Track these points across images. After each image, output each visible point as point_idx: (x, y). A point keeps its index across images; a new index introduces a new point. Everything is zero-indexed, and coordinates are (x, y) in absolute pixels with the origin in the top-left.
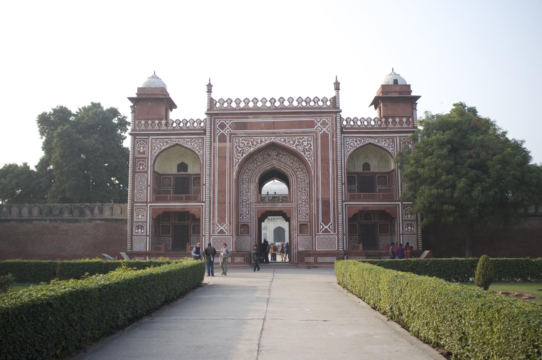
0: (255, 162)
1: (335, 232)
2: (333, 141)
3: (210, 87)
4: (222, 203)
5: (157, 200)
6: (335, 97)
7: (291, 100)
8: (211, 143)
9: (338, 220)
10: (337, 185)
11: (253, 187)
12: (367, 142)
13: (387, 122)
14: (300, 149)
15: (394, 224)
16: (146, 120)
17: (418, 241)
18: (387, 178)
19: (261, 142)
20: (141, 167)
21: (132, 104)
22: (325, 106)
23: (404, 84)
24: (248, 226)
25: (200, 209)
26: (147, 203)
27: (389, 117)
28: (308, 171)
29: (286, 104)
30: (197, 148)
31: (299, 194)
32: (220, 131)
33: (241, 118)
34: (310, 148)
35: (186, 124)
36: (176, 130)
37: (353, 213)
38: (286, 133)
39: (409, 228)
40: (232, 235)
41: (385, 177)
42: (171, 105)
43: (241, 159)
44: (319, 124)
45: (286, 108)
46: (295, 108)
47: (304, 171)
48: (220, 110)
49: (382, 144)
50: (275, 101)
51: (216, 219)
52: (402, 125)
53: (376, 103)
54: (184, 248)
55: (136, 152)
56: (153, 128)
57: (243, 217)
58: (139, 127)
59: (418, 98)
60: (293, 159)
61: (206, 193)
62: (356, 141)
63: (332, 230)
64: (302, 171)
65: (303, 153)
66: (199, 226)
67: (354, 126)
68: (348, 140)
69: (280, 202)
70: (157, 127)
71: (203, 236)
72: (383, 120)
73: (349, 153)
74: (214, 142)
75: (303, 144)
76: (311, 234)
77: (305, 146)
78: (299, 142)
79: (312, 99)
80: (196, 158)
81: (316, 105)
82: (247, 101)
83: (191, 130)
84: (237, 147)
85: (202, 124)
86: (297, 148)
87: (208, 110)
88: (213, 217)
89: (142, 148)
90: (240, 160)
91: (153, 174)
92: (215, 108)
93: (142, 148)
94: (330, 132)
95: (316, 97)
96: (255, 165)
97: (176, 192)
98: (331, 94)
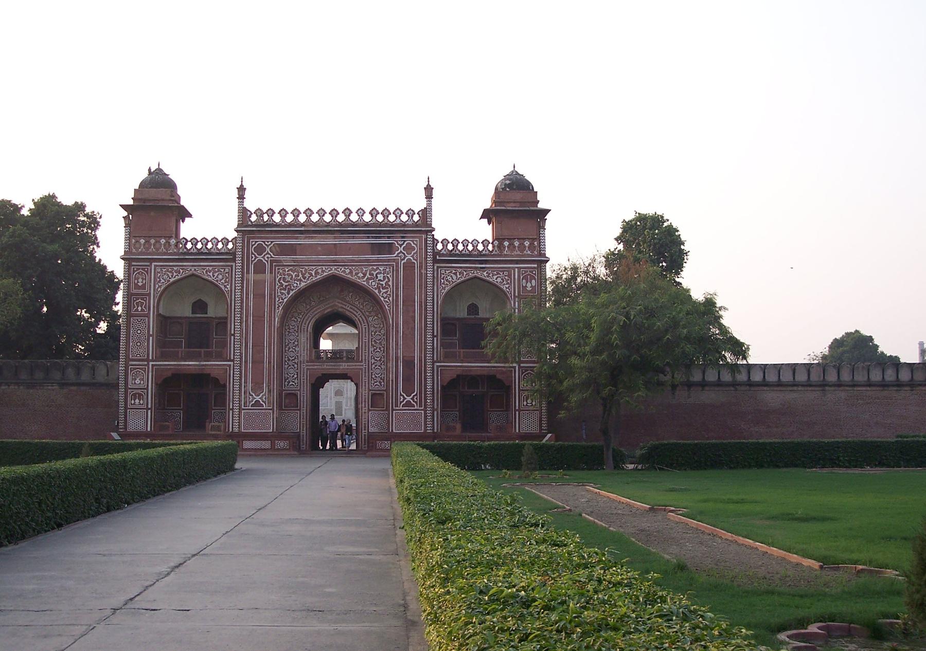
3: (241, 190)
4: (258, 362)
5: (163, 356)
8: (243, 275)
9: (426, 388)
11: (304, 339)
12: (471, 275)
13: (501, 246)
14: (372, 285)
16: (148, 238)
17: (541, 421)
20: (140, 308)
21: (125, 214)
24: (296, 395)
27: (504, 239)
28: (385, 318)
29: (354, 218)
32: (256, 257)
35: (207, 244)
36: (192, 254)
38: (353, 261)
42: (184, 214)
45: (354, 224)
49: (494, 279)
51: (250, 385)
52: (522, 251)
54: (201, 426)
55: (132, 285)
56: (157, 250)
58: (137, 249)
61: (235, 347)
65: (376, 291)
71: (230, 409)
74: (248, 272)
76: (387, 409)
81: (398, 221)
85: (230, 246)
86: (368, 283)
87: (239, 225)
89: (140, 280)
93: (140, 280)
97: (189, 346)
98: (419, 204)
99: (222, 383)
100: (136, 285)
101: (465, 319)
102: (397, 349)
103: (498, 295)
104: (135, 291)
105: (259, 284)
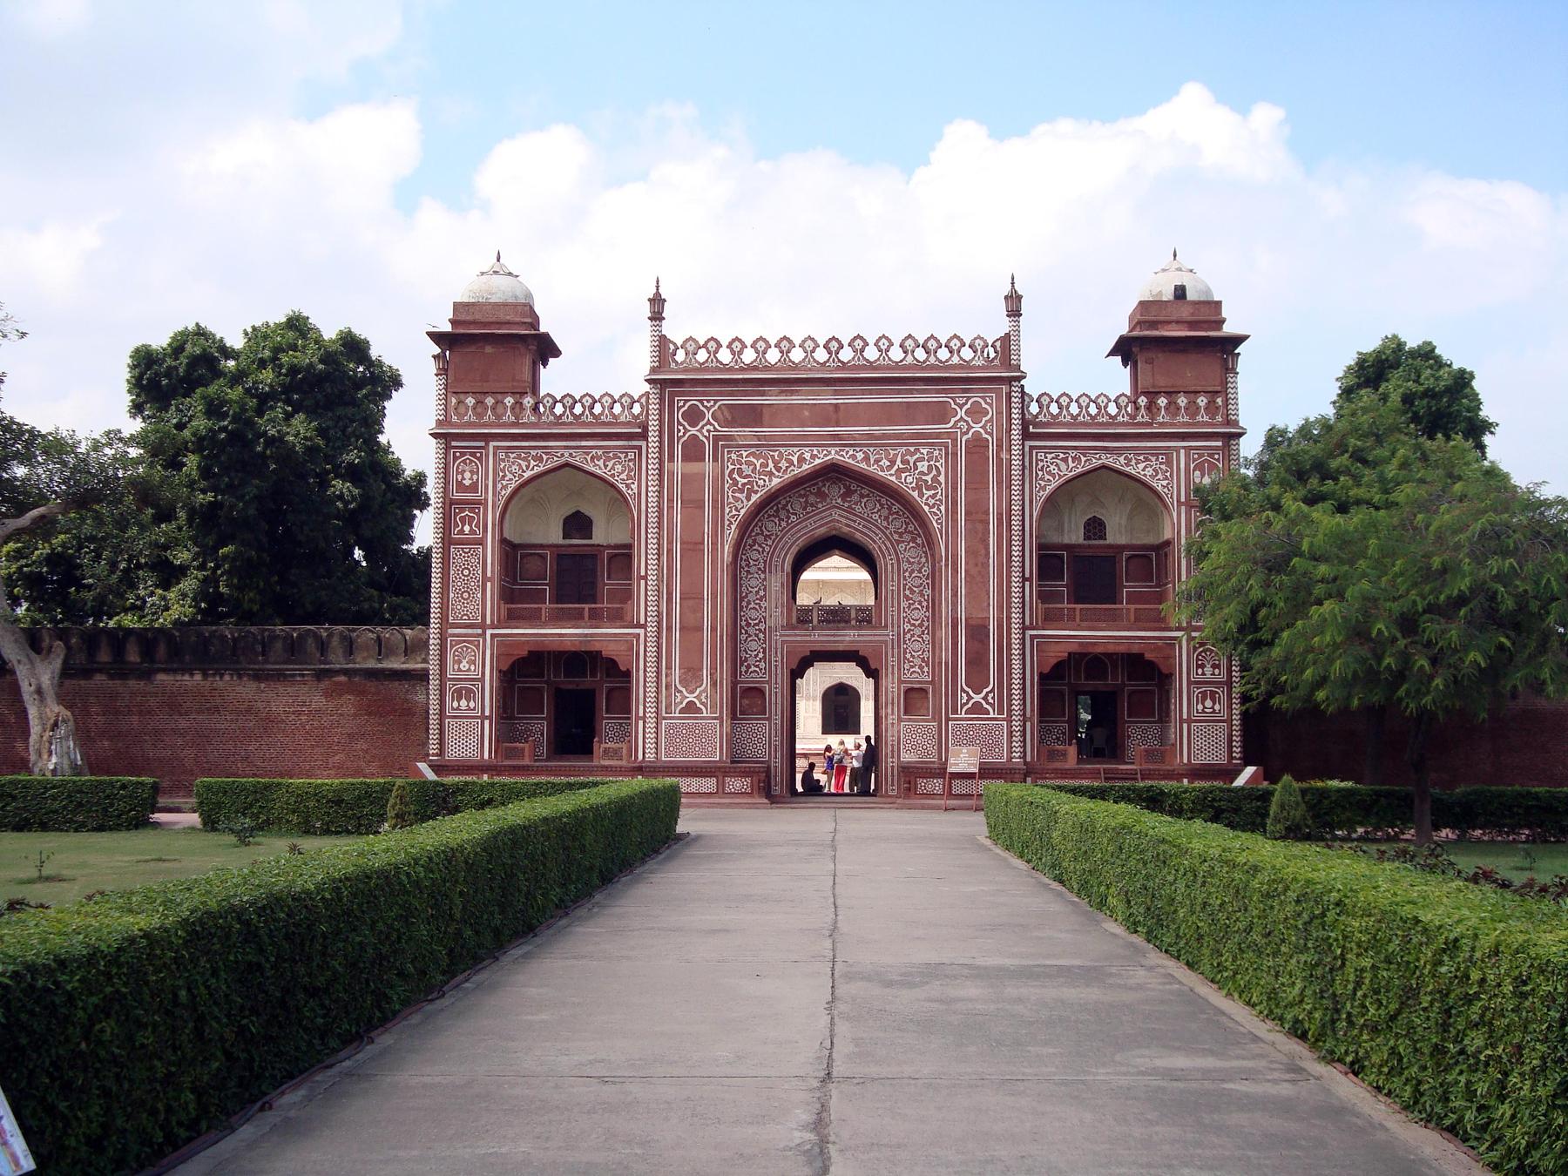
0: (783, 514)
2: (1000, 460)
3: (657, 302)
4: (691, 629)
5: (512, 618)
6: (1008, 335)
7: (884, 344)
8: (661, 463)
10: (1009, 582)
11: (777, 582)
12: (1096, 463)
13: (1151, 407)
14: (907, 483)
15: (1168, 692)
16: (480, 395)
17: (1230, 741)
18: (1152, 560)
19: (801, 460)
20: (467, 528)
21: (437, 350)
22: (981, 363)
23: (1202, 299)
24: (761, 692)
25: (630, 644)
26: (483, 626)
28: (930, 542)
29: (871, 354)
30: (624, 476)
33: (746, 394)
34: (935, 479)
36: (564, 424)
37: (1054, 661)
38: (871, 436)
39: (1208, 703)
40: (720, 718)
41: (1149, 558)
42: (546, 349)
44: (961, 413)
45: (871, 366)
46: (897, 366)
47: (919, 541)
48: (686, 370)
49: (1139, 469)
50: (841, 347)
51: (677, 673)
52: (1193, 415)
53: (1125, 349)
54: (586, 750)
55: (453, 486)
56: (499, 417)
57: (748, 667)
59: (1238, 340)
60: (889, 509)
62: (1065, 460)
63: (992, 705)
64: (913, 540)
65: (915, 494)
66: (628, 690)
67: (1061, 418)
68: (1041, 456)
69: (853, 628)
70: (509, 417)
72: (1143, 401)
73: (1045, 494)
74: (671, 459)
79: (943, 342)
80: (618, 501)
81: (955, 360)
82: (761, 345)
83: (604, 424)
85: (637, 409)
86: (899, 478)
87: (653, 370)
88: (669, 667)
89: (467, 475)
90: (743, 512)
91: (501, 548)
92: (673, 365)
93: (467, 475)
94: (991, 434)
95: (955, 336)
96: (784, 524)
98: (999, 325)
99: (623, 668)
100: (459, 484)
101: (1079, 546)
102: (956, 604)
103: (1145, 498)
104: (457, 496)
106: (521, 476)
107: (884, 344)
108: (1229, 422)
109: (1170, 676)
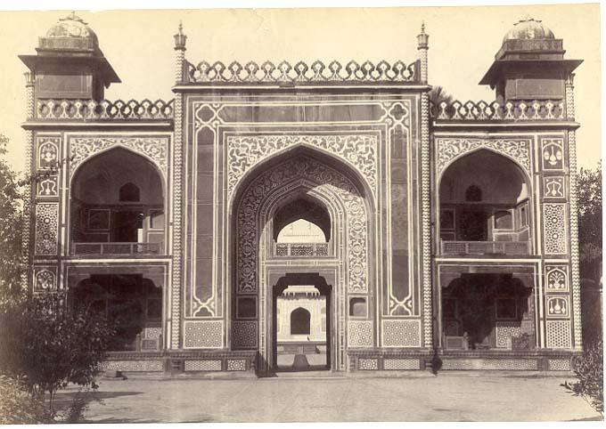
0: (267, 183)
1: (417, 313)
6: (419, 61)
7: (335, 67)
9: (422, 291)
14: (351, 160)
19: (280, 143)
20: (48, 191)
21: (29, 70)
25: (162, 268)
27: (518, 101)
30: (158, 155)
31: (349, 242)
34: (370, 157)
42: (104, 75)
43: (241, 174)
46: (344, 82)
52: (543, 116)
57: (244, 284)
58: (44, 115)
59: (575, 64)
63: (411, 309)
65: (357, 167)
75: (357, 149)
77: (361, 153)
78: (349, 145)
81: (384, 77)
84: (235, 154)
85: (167, 111)
86: (346, 155)
89: (48, 155)
90: (240, 179)
93: (48, 155)
105: (205, 158)
106: (86, 156)
107: (335, 67)
108: (566, 120)
109: (531, 288)
